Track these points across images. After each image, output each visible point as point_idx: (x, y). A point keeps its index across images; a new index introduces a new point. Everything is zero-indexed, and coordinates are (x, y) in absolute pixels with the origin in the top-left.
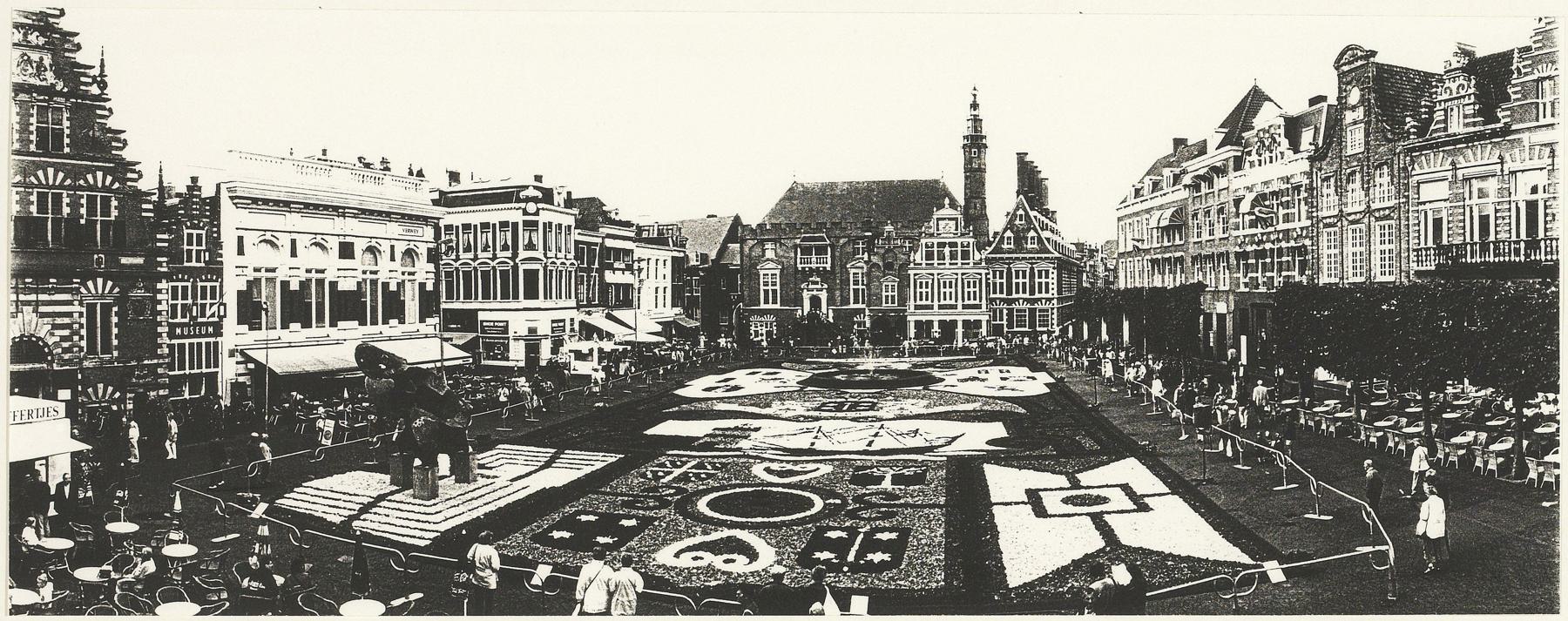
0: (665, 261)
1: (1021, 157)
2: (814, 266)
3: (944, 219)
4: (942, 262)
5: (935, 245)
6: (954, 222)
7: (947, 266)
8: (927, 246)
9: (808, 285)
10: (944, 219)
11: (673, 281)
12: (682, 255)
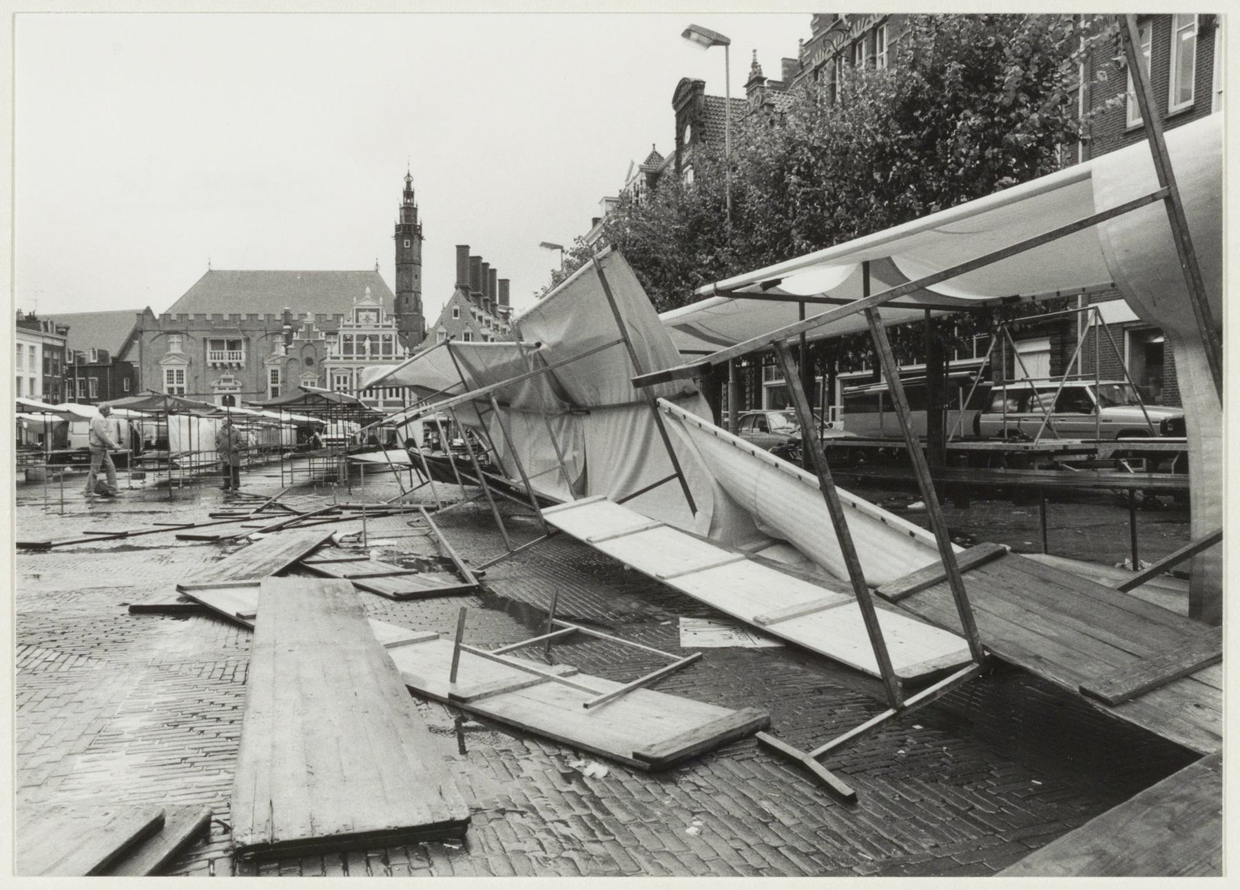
0: (32, 348)
1: (462, 250)
2: (226, 361)
3: (364, 310)
4: (361, 356)
5: (355, 338)
6: (375, 314)
7: (368, 359)
8: (346, 339)
10: (364, 310)
11: (46, 369)
12: (60, 344)
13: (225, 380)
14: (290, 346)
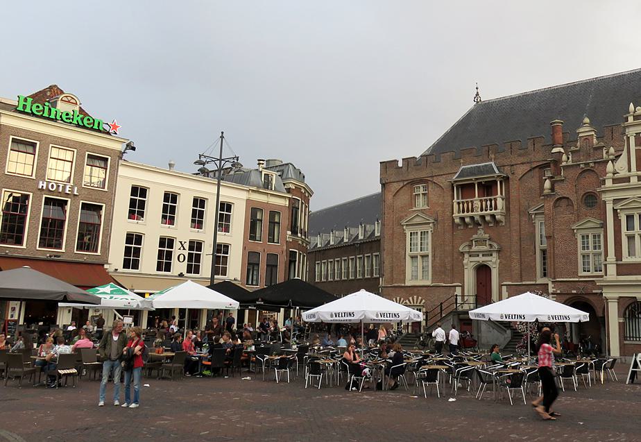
9: (470, 246)
13: (479, 242)
14: (557, 178)
